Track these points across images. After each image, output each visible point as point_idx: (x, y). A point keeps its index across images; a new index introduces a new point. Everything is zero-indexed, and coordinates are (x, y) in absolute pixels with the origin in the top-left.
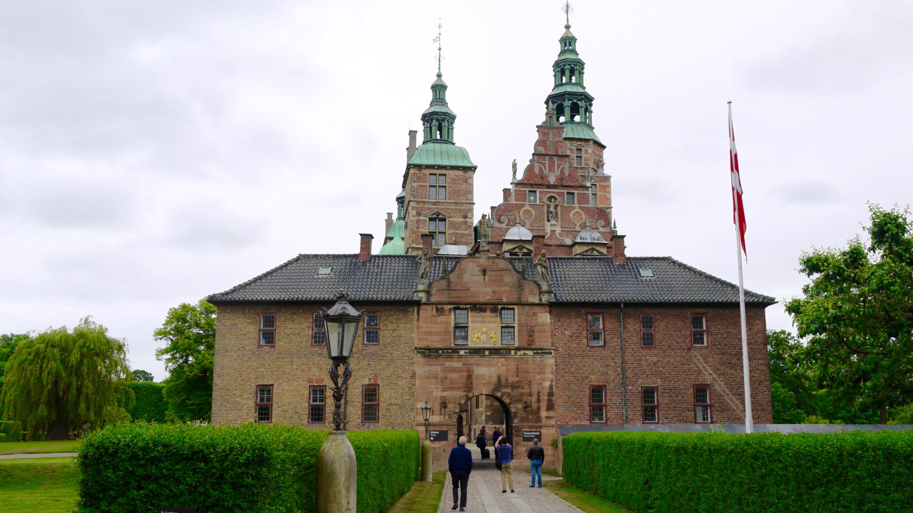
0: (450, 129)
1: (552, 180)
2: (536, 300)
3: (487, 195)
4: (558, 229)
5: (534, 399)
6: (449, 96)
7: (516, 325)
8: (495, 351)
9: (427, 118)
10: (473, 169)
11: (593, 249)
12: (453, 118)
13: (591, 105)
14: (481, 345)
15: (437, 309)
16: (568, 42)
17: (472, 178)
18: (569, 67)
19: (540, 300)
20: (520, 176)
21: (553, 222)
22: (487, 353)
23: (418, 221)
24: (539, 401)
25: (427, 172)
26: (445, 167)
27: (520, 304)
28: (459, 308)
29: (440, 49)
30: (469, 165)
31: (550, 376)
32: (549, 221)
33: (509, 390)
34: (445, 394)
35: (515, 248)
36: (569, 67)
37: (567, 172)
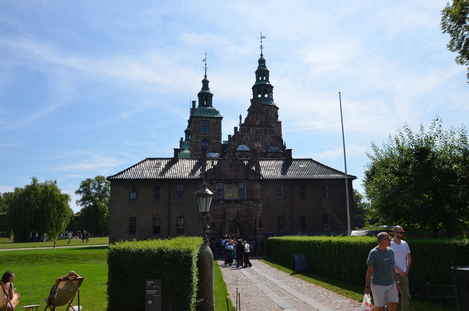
1: (257, 123)
2: (254, 178)
3: (228, 130)
4: (260, 146)
5: (253, 222)
6: (210, 85)
7: (245, 190)
8: (236, 201)
11: (276, 155)
12: (212, 95)
13: (272, 90)
14: (230, 199)
15: (210, 183)
16: (262, 62)
17: (221, 122)
19: (256, 178)
20: (243, 122)
21: (258, 143)
22: (232, 202)
23: (197, 142)
24: (255, 223)
25: (200, 119)
26: (209, 118)
27: (246, 179)
28: (219, 182)
29: (206, 64)
31: (260, 212)
33: (242, 219)
34: (214, 221)
36: (262, 72)
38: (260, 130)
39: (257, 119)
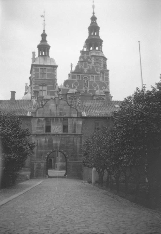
0: (48, 51)
1: (86, 71)
3: (62, 77)
6: (48, 39)
9: (40, 47)
10: (56, 67)
16: (94, 19)
17: (56, 70)
18: (94, 28)
20: (74, 69)
25: (39, 67)
29: (44, 21)
30: (55, 65)
32: (84, 86)
35: (71, 97)
36: (94, 28)
37: (91, 69)
38: (88, 76)
39: (85, 67)
